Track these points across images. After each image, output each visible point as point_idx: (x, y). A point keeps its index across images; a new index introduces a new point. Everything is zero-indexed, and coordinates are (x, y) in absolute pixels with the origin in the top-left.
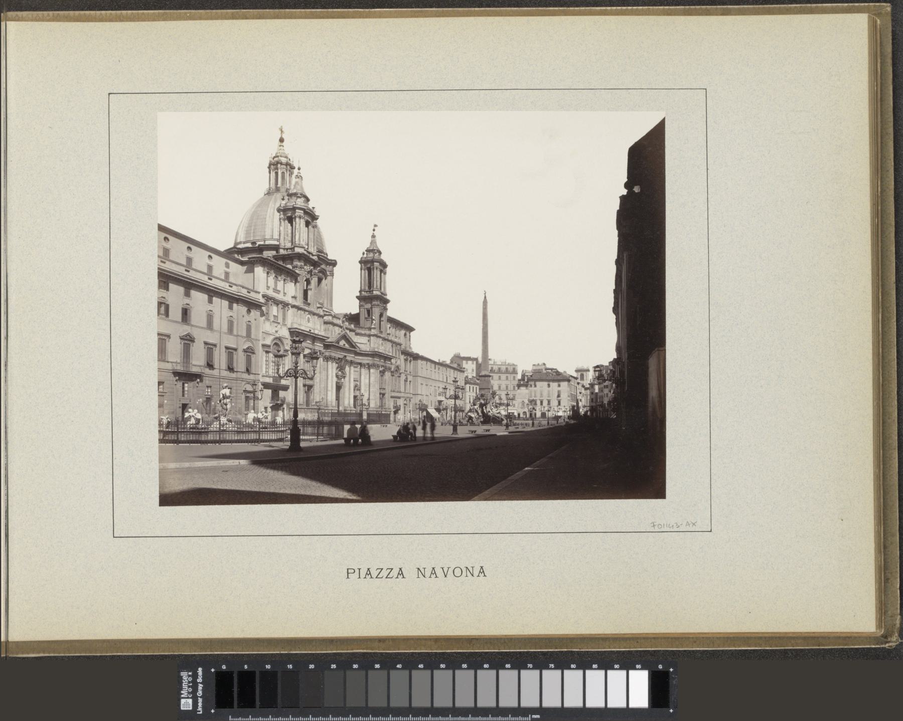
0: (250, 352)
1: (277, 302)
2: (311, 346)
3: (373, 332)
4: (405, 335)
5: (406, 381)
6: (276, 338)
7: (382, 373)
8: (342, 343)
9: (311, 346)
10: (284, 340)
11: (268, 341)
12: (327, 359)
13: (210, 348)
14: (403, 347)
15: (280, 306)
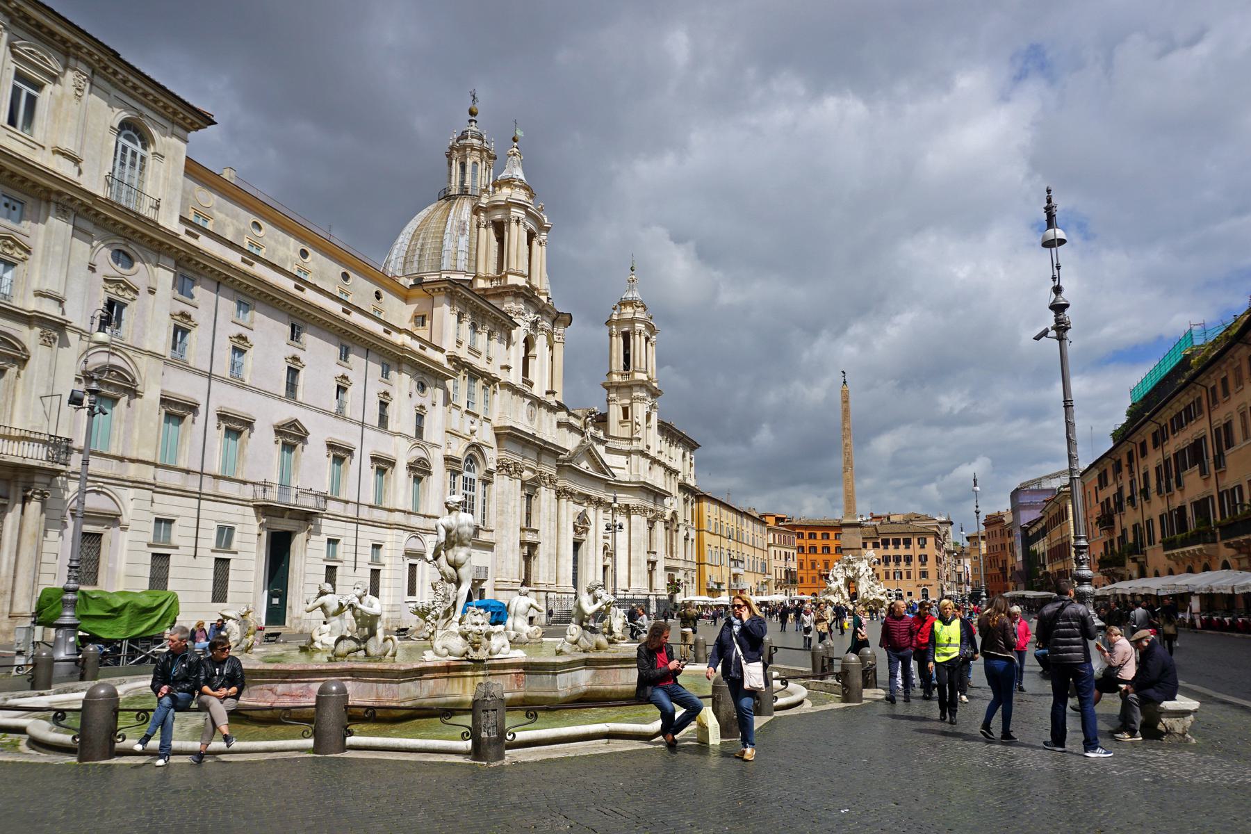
0: (419, 470)
1: (475, 375)
2: (533, 465)
3: (636, 445)
4: (684, 456)
5: (686, 539)
6: (473, 446)
7: (651, 524)
8: (584, 465)
9: (533, 465)
10: (486, 450)
11: (458, 449)
12: (561, 493)
13: (340, 453)
14: (680, 477)
15: (480, 383)
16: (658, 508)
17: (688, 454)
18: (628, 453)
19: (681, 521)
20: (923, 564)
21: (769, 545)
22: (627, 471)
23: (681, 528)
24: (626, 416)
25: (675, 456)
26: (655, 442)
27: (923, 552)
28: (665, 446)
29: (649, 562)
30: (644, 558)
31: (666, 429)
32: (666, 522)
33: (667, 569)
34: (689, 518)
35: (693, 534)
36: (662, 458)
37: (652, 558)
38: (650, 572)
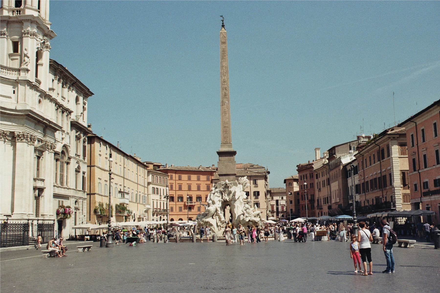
3: (23, 76)
16: (48, 139)
17: (81, 98)
18: (15, 83)
19: (72, 153)
20: (257, 198)
21: (149, 184)
22: (13, 100)
23: (73, 161)
24: (16, 50)
25: (68, 97)
26: (47, 80)
27: (256, 190)
28: (58, 86)
29: (35, 189)
30: (30, 184)
31: (56, 69)
32: (56, 153)
33: (56, 196)
34: (81, 153)
35: (84, 168)
36: (54, 95)
37: (39, 184)
38: (37, 198)
